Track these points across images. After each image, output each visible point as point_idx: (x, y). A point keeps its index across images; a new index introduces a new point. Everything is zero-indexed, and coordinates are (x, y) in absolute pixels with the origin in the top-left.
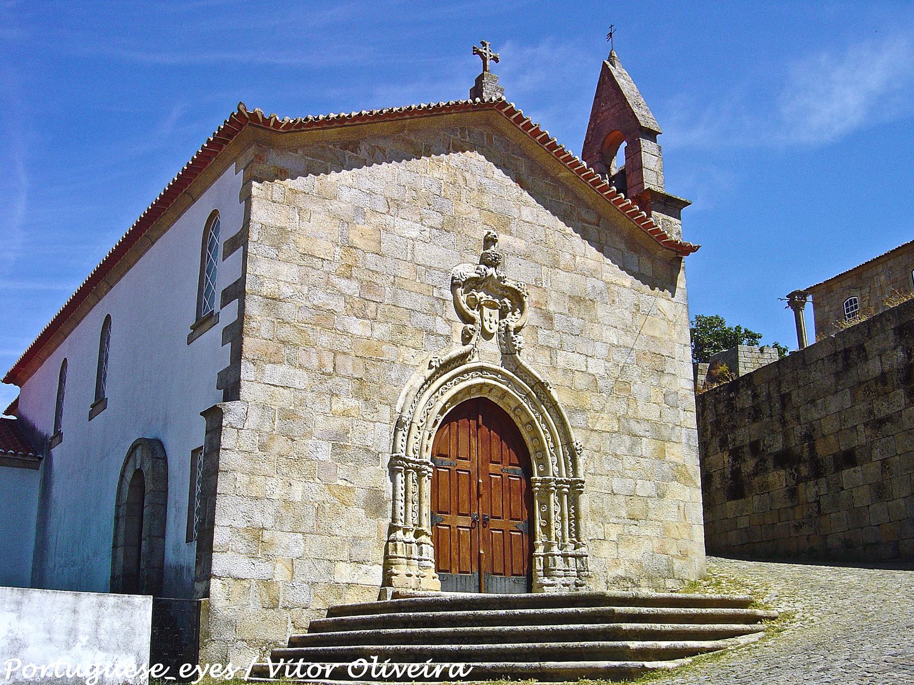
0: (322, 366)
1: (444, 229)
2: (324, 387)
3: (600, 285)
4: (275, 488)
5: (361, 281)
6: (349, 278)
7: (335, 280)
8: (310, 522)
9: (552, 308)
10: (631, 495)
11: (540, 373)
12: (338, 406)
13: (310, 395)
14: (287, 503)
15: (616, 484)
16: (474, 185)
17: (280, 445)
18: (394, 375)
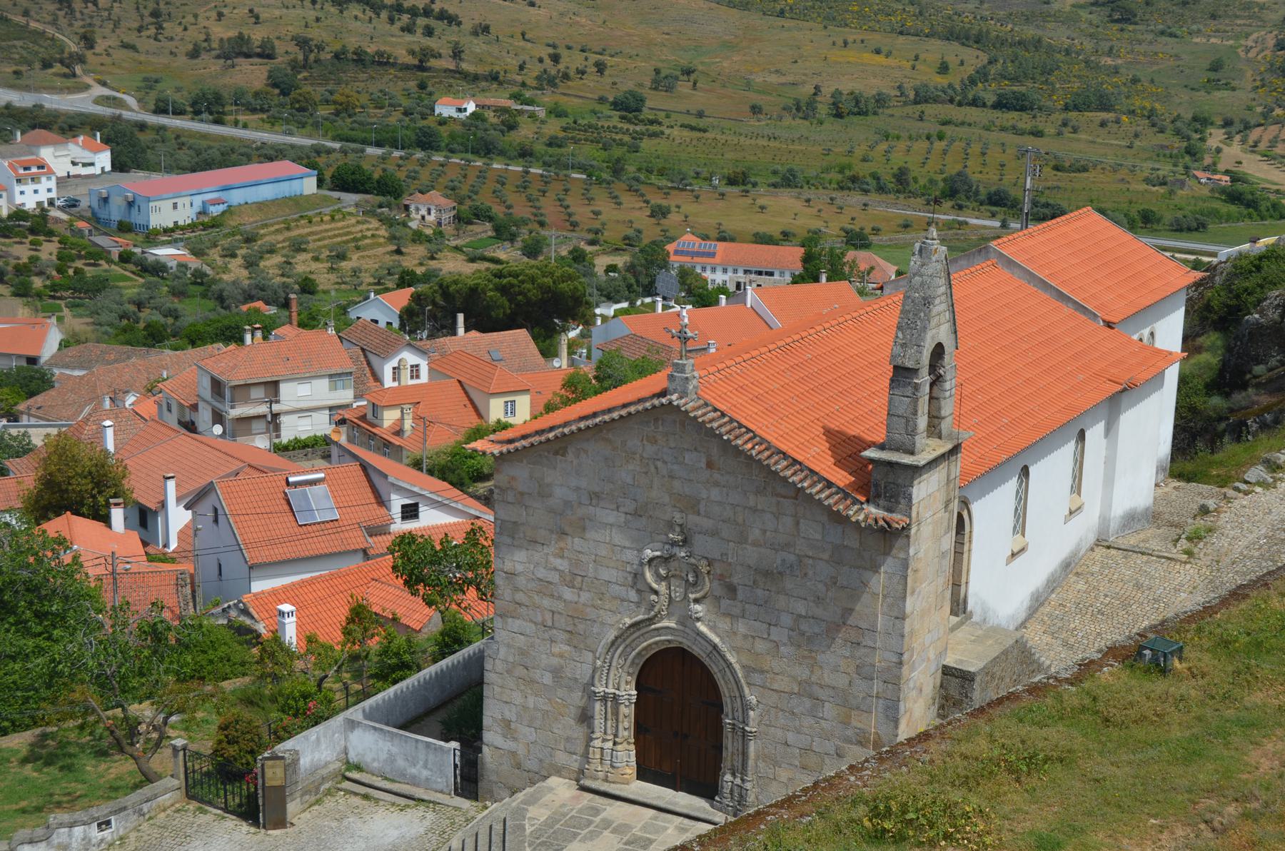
0: (544, 620)
1: (636, 514)
2: (546, 636)
3: (792, 558)
4: (517, 698)
5: (570, 559)
6: (562, 557)
7: (551, 559)
8: (538, 723)
9: (735, 580)
10: (806, 750)
11: (719, 636)
12: (556, 650)
13: (538, 641)
14: (525, 708)
15: (791, 737)
16: (665, 472)
17: (520, 671)
18: (595, 630)
